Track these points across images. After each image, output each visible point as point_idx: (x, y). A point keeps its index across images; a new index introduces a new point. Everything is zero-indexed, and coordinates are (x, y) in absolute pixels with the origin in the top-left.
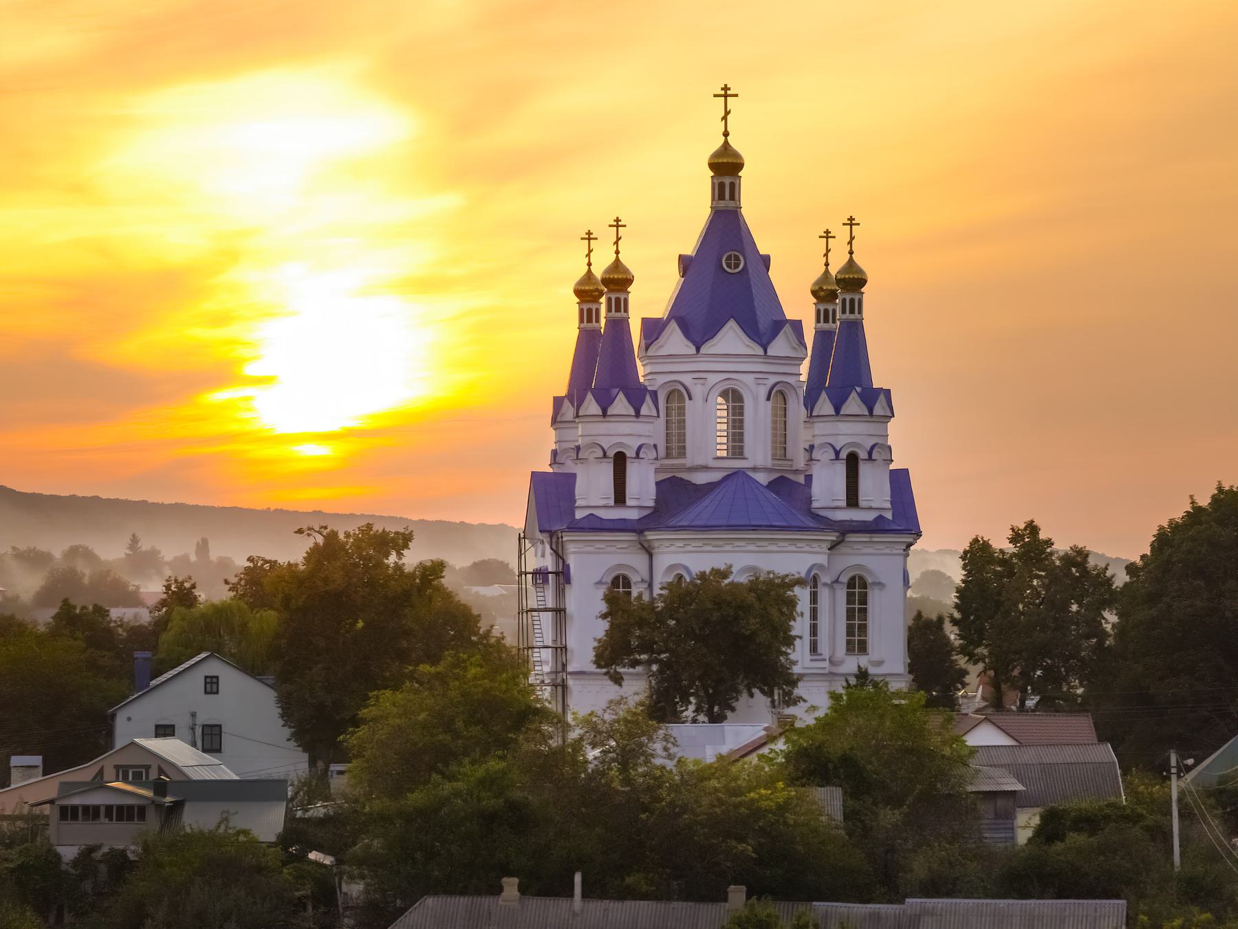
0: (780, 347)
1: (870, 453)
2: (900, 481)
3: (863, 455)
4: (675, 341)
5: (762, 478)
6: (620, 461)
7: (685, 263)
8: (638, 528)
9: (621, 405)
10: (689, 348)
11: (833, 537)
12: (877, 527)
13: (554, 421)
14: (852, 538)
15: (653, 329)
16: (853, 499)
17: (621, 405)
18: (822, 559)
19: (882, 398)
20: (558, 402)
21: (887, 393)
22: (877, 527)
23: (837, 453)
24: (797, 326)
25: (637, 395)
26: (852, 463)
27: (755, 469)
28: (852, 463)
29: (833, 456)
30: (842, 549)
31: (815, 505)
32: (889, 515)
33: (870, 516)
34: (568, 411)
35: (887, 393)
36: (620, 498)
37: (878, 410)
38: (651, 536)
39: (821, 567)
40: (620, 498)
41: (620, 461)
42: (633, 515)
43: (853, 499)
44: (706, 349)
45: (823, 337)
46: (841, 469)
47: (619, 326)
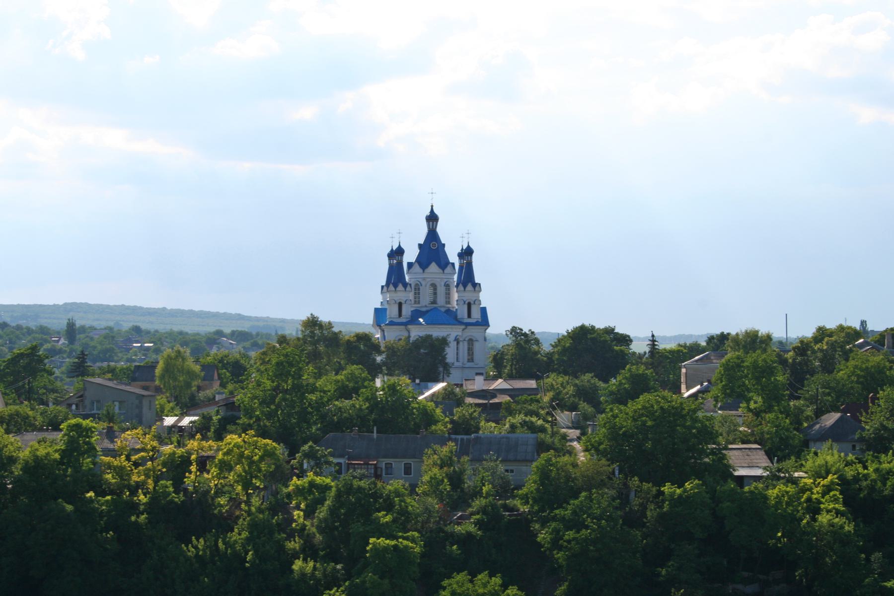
0: (448, 269)
1: (474, 302)
2: (484, 311)
3: (472, 303)
4: (417, 268)
5: (443, 310)
6: (400, 305)
7: (420, 246)
8: (405, 324)
9: (400, 287)
10: (420, 270)
11: (463, 327)
12: (476, 324)
13: (382, 293)
14: (469, 327)
15: (410, 265)
16: (469, 316)
17: (400, 287)
18: (460, 334)
19: (478, 285)
20: (382, 287)
21: (480, 284)
22: (476, 324)
23: (465, 302)
24: (453, 264)
25: (405, 285)
26: (469, 305)
27: (441, 307)
28: (469, 305)
29: (463, 303)
30: (466, 330)
31: (458, 317)
32: (480, 320)
33: (474, 321)
34: (385, 288)
35: (480, 284)
36: (400, 315)
37: (477, 288)
38: (409, 327)
39: (460, 336)
40: (400, 315)
41: (400, 305)
42: (404, 320)
43: (469, 316)
44: (427, 271)
45: (461, 267)
46: (466, 307)
47: (400, 263)
